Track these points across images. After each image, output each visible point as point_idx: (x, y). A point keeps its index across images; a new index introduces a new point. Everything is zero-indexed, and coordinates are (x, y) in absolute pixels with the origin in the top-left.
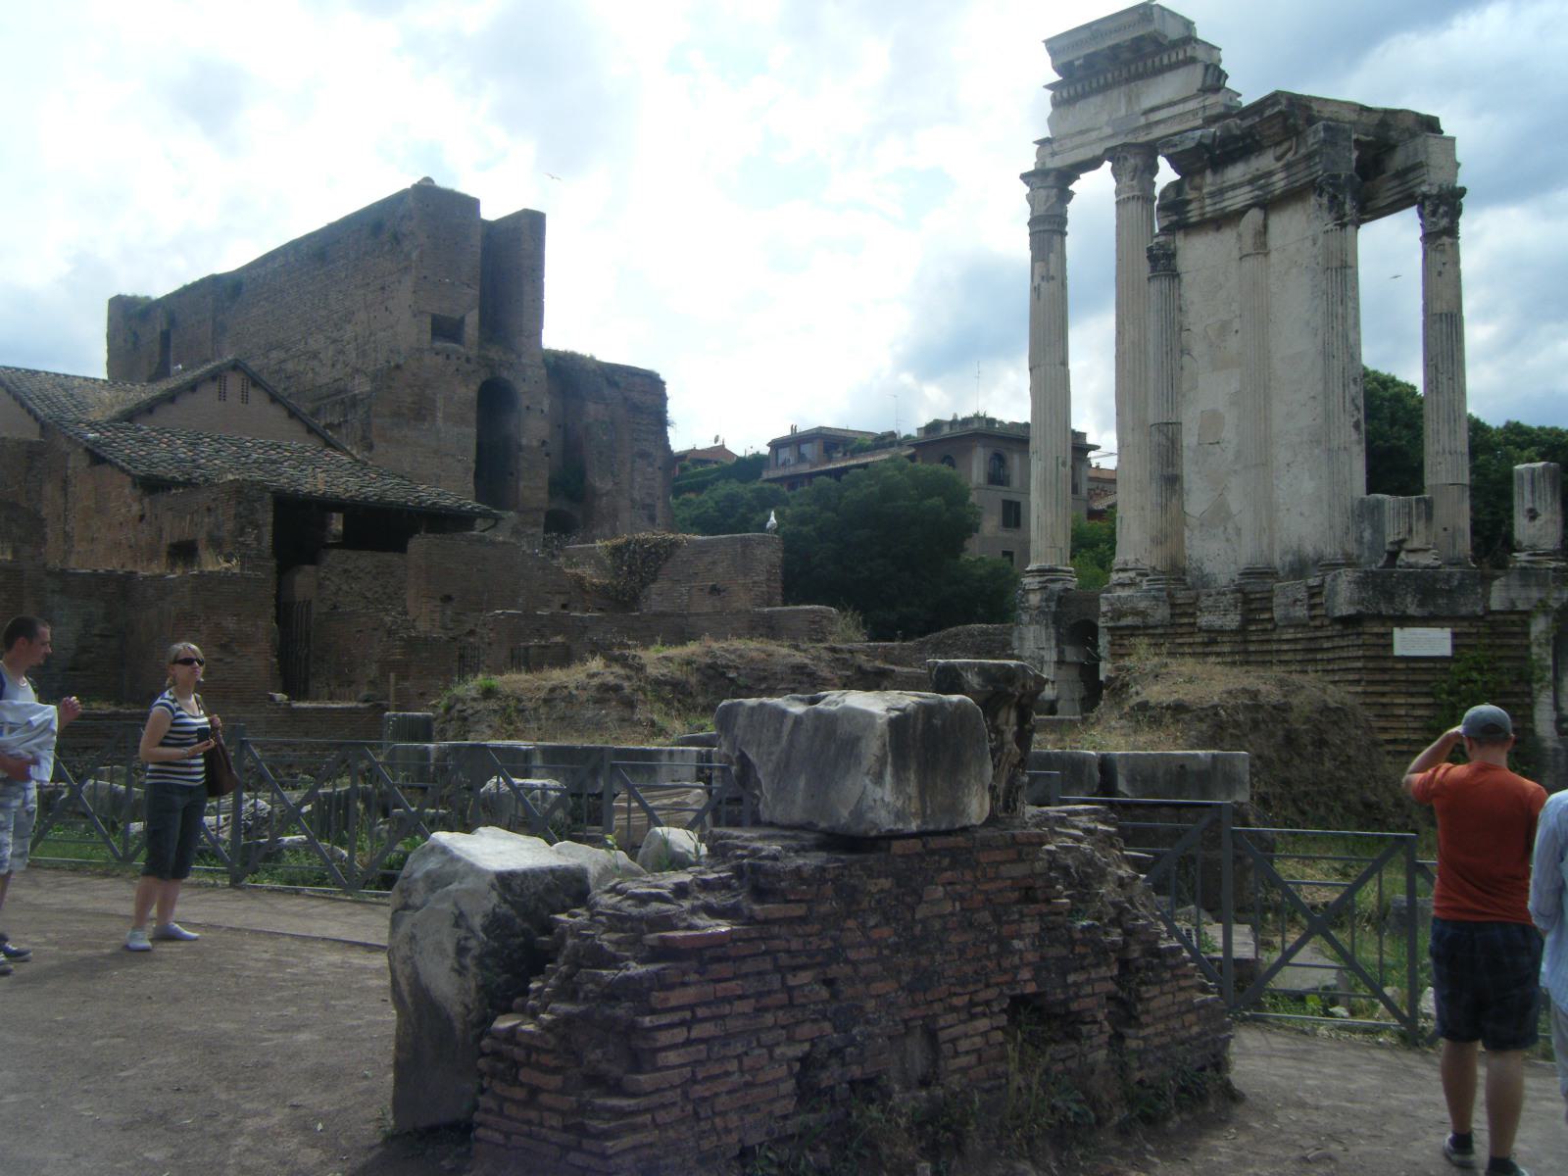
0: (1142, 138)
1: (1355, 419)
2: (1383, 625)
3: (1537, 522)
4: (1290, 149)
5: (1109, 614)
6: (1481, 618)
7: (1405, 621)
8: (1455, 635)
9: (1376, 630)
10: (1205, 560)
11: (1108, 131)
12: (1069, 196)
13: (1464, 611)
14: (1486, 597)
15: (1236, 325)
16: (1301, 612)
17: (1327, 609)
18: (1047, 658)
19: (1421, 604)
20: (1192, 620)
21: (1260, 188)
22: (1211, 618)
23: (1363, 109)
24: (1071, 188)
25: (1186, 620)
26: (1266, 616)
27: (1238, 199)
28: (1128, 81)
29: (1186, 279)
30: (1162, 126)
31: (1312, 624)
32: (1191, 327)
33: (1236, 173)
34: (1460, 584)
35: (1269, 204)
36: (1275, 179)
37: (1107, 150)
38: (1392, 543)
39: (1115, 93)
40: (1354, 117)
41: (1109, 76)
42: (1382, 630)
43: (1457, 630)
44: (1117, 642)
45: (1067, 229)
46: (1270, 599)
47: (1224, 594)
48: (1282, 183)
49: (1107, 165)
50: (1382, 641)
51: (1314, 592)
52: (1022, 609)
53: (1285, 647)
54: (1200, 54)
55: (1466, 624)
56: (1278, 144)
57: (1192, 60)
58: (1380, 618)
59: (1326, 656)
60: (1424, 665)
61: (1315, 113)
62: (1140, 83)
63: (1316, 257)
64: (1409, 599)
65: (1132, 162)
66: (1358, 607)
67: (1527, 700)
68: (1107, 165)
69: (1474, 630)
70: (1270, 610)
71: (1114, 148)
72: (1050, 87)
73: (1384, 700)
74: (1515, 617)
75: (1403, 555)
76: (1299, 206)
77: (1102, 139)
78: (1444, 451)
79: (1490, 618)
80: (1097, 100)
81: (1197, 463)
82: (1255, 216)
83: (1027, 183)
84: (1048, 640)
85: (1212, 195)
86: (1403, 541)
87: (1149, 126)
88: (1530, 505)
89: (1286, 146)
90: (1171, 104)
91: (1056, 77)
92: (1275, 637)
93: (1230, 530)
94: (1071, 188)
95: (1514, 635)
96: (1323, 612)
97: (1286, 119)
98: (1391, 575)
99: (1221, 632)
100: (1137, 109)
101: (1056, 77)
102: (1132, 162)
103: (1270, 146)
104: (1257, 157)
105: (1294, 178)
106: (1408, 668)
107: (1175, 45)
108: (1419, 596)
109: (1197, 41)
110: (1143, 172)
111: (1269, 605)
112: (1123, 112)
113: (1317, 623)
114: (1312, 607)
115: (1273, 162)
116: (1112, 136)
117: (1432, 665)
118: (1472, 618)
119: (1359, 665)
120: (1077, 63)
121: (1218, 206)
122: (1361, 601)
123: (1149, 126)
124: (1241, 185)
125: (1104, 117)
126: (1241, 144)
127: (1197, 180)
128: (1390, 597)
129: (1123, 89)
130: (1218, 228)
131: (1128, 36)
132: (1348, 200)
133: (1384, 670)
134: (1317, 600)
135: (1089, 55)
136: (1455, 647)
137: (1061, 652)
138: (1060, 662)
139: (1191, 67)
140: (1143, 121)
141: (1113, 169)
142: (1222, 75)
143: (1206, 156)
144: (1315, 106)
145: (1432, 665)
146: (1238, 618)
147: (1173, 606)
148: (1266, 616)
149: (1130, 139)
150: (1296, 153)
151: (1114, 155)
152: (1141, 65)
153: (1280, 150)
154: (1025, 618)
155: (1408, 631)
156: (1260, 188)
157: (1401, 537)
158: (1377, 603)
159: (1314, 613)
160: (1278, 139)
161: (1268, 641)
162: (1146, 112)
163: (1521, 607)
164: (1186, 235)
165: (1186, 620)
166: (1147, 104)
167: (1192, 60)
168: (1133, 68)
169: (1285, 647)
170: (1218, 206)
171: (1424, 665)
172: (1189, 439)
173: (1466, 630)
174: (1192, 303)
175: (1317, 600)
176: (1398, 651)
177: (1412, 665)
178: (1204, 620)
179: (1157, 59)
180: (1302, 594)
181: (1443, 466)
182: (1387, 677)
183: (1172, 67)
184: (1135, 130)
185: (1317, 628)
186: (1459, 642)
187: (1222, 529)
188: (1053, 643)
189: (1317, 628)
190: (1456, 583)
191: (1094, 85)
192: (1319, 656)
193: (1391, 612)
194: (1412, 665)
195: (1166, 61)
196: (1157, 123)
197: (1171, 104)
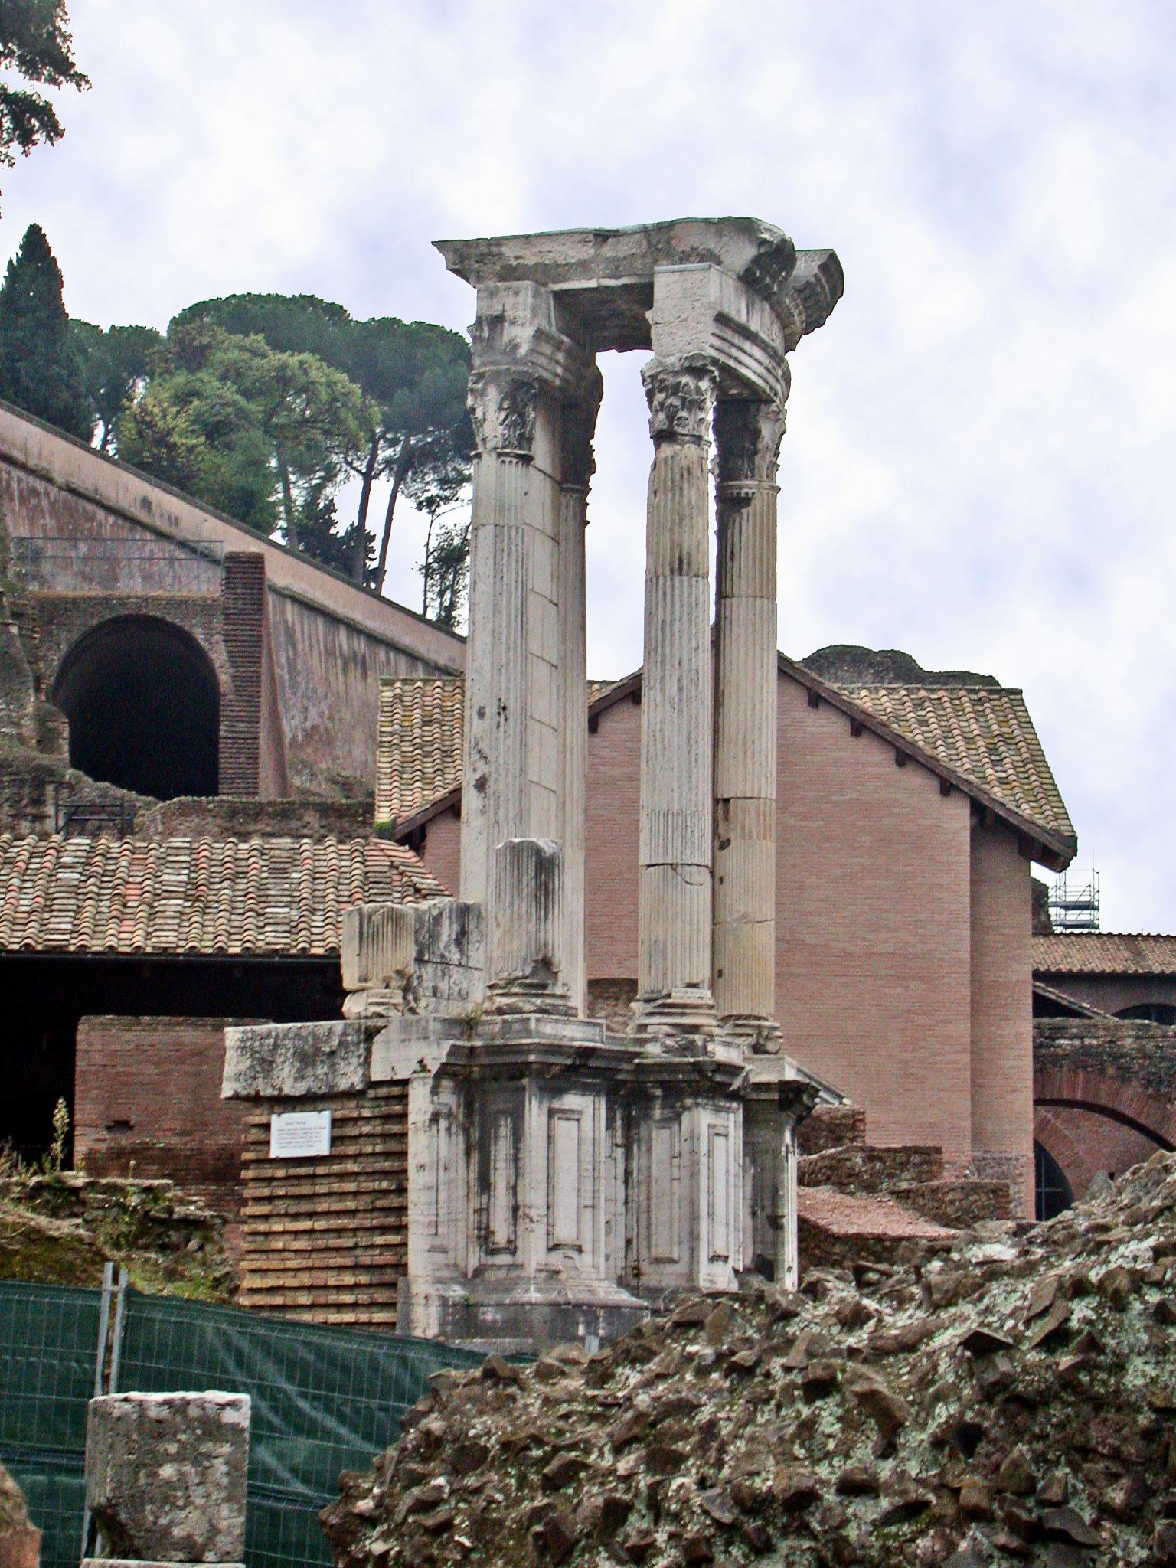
1: (478, 775)
6: (361, 1094)
8: (335, 1122)
13: (343, 1085)
19: (300, 1077)
34: (341, 1044)
42: (264, 1120)
43: (339, 1114)
58: (256, 1100)
60: (302, 1171)
64: (287, 1067)
73: (263, 1227)
79: (371, 1093)
117: (309, 1170)
118: (350, 1094)
136: (335, 1141)
155: (287, 1117)
158: (255, 1078)
163: (401, 1075)
171: (302, 1171)
176: (275, 1152)
182: (266, 1192)
186: (338, 1132)
190: (337, 1042)
193: (268, 1092)
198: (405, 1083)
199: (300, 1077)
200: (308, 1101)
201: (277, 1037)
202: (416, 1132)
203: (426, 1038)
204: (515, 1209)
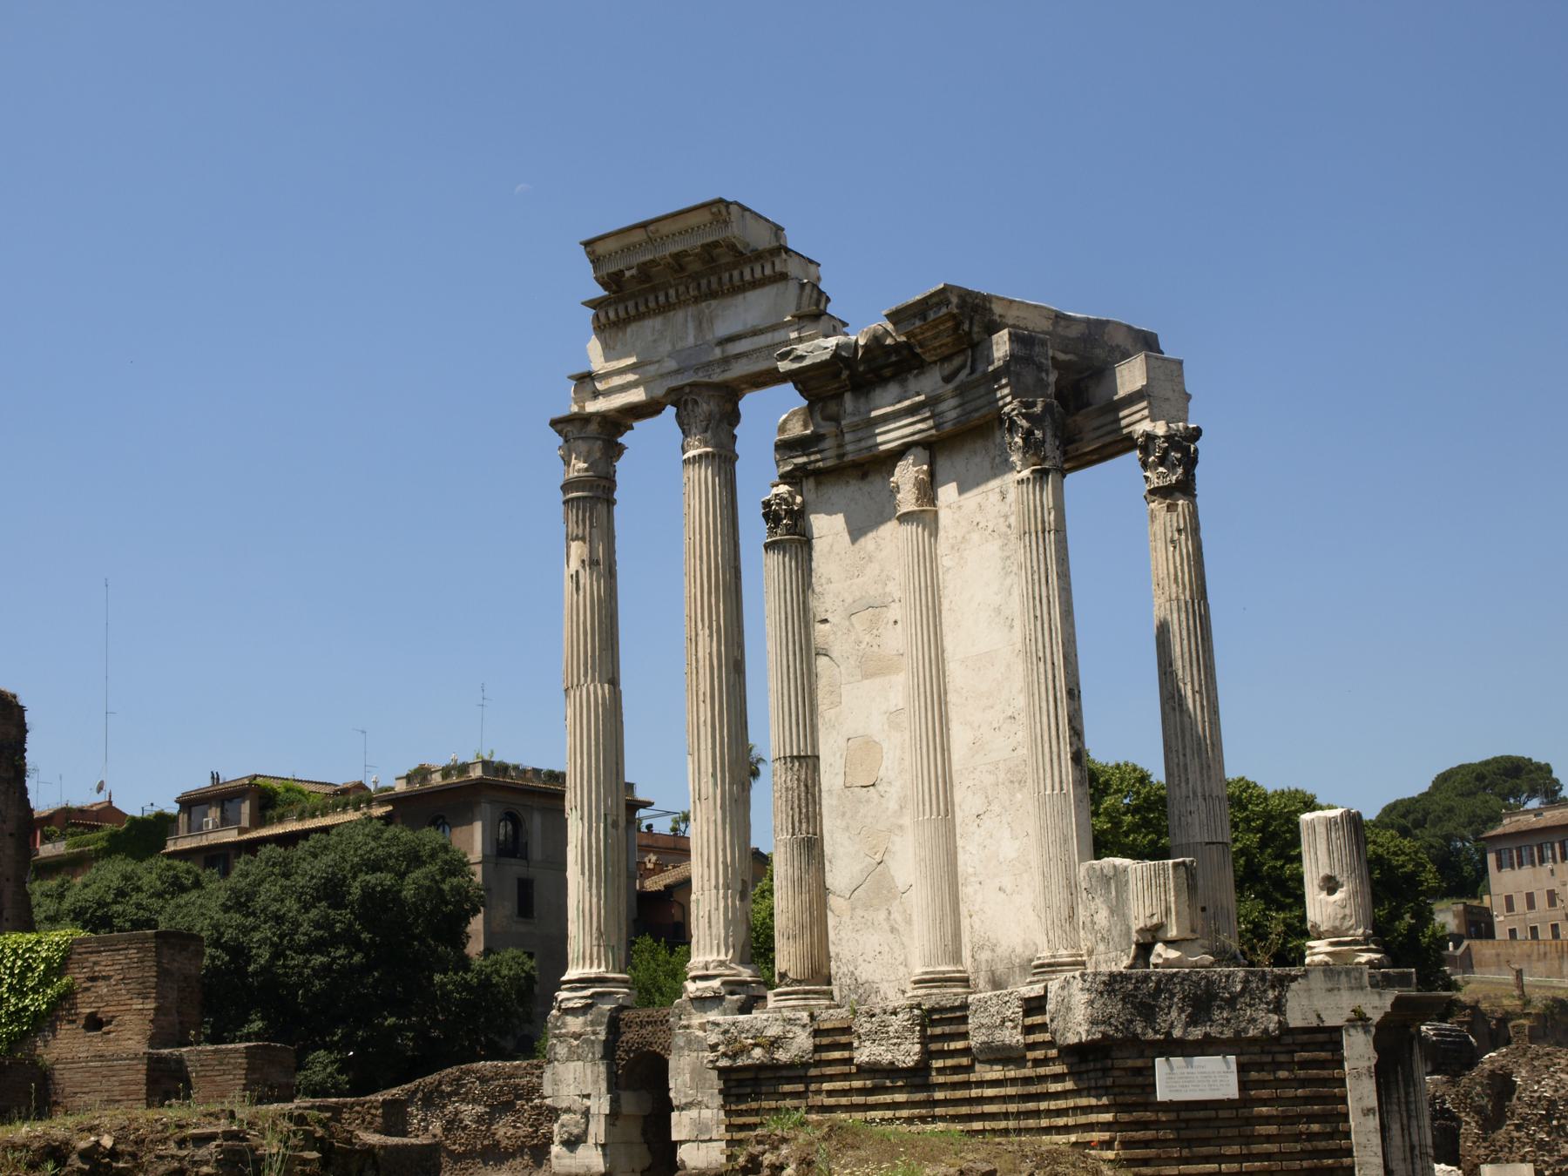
0: (717, 377)
2: (1141, 1055)
3: (1339, 895)
4: (963, 367)
5: (722, 1048)
6: (1277, 1039)
7: (1173, 1047)
8: (1242, 1069)
9: (1130, 1063)
10: (860, 960)
11: (671, 365)
12: (619, 450)
14: (1278, 1007)
15: (895, 612)
16: (1012, 1036)
17: (1054, 1033)
18: (593, 1110)
19: (1193, 1021)
20: (846, 1054)
22: (876, 1049)
23: (1059, 317)
24: (620, 440)
25: (837, 1055)
26: (960, 1045)
28: (697, 300)
30: (744, 360)
31: (1030, 1055)
32: (829, 616)
36: (943, 407)
37: (671, 391)
38: (1141, 931)
39: (679, 315)
40: (1046, 325)
41: (672, 292)
42: (1139, 1063)
43: (1245, 1059)
44: (734, 1091)
45: (616, 495)
46: (964, 1020)
47: (895, 1013)
48: (953, 414)
49: (670, 411)
50: (1140, 1080)
51: (1034, 1005)
52: (556, 1036)
53: (989, 1092)
54: (793, 268)
55: (1257, 1049)
57: (783, 277)
58: (1134, 1043)
59: (1053, 1105)
60: (1201, 1114)
61: (996, 318)
62: (714, 303)
63: (1006, 517)
65: (705, 407)
66: (1102, 1028)
67: (1347, 1161)
68: (670, 411)
69: (1269, 1059)
70: (965, 1036)
71: (681, 388)
72: (594, 304)
74: (1321, 1037)
75: (1159, 948)
77: (662, 376)
78: (1195, 793)
79: (1288, 1039)
80: (655, 323)
81: (844, 814)
83: (560, 433)
84: (596, 1082)
85: (855, 428)
86: (1160, 927)
87: (726, 361)
88: (1327, 871)
89: (957, 362)
90: (755, 333)
91: (599, 292)
92: (973, 1077)
93: (896, 916)
94: (620, 440)
95: (1321, 1064)
96: (1047, 1037)
97: (958, 326)
98: (1147, 978)
99: (892, 1071)
100: (709, 337)
101: (599, 292)
102: (705, 407)
103: (935, 362)
104: (916, 376)
105: (969, 407)
106: (1178, 1120)
107: (759, 256)
108: (1189, 1010)
109: (787, 251)
110: (720, 421)
111: (962, 1028)
112: (691, 340)
113: (1039, 1054)
115: (941, 383)
116: (677, 372)
117: (1212, 1114)
119: (1108, 1117)
120: (628, 274)
121: (863, 444)
122: (1106, 1021)
123: (726, 361)
125: (665, 347)
126: (894, 359)
127: (832, 408)
128: (1147, 1011)
129: (692, 310)
130: (864, 476)
131: (695, 242)
132: (1049, 439)
133: (1145, 1125)
134: (1038, 1019)
135: (644, 264)
136: (1243, 1085)
137: (614, 1103)
138: (613, 1117)
139: (780, 286)
140: (718, 352)
141: (678, 416)
142: (821, 297)
143: (845, 374)
144: (997, 309)
145: (1212, 1114)
146: (917, 1048)
147: (817, 1033)
148: (960, 1045)
149: (700, 377)
150: (973, 371)
151: (681, 399)
152: (714, 280)
153: (948, 368)
154: (561, 1050)
157: (1155, 920)
158: (1131, 1021)
159: (1031, 1038)
160: (947, 352)
161: (967, 1085)
162: (724, 341)
164: (818, 484)
165: (837, 1055)
166: (722, 329)
167: (783, 277)
168: (704, 282)
169: (989, 1092)
170: (863, 444)
171: (1201, 1114)
172: (830, 777)
173: (1256, 1058)
174: (830, 581)
175: (1038, 1019)
177: (1183, 1115)
178: (865, 1053)
179: (736, 273)
180: (1015, 1010)
181: (1195, 816)
183: (756, 284)
184: (710, 364)
185: (1037, 1063)
187: (882, 915)
188: (603, 1086)
189: (1037, 1063)
190: (1239, 988)
191: (652, 305)
192: (1043, 1105)
193: (1150, 1035)
194: (1183, 1115)
195: (747, 276)
196: (738, 356)
197: (755, 333)
198: (1338, 1029)
199: (1193, 1021)
200: (1206, 1046)
201: (1158, 982)
202: (1359, 1076)
203: (1362, 988)
204: (1412, 1148)
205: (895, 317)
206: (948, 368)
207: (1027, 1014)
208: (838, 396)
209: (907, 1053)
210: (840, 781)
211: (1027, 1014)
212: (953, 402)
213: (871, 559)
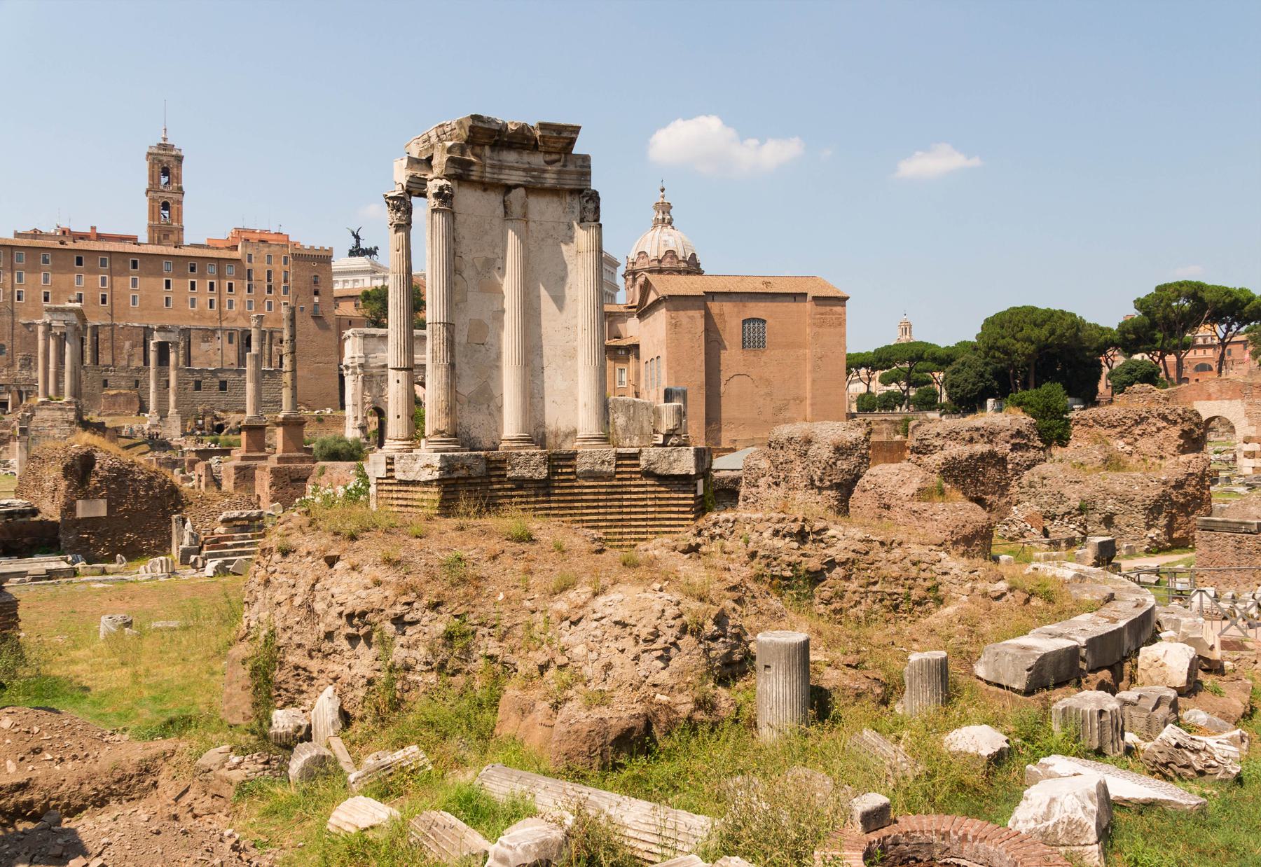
4: (559, 160)
21: (533, 177)
26: (569, 470)
27: (513, 177)
29: (459, 218)
33: (510, 157)
35: (533, 189)
36: (547, 175)
46: (574, 459)
56: (550, 153)
59: (634, 496)
76: (556, 199)
82: (521, 191)
89: (554, 157)
99: (531, 480)
114: (617, 466)
124: (517, 169)
130: (485, 190)
148: (569, 470)
153: (549, 158)
156: (533, 177)
172: (461, 338)
185: (619, 479)
205: (543, 126)
206: (549, 158)
207: (618, 459)
208: (483, 145)
209: (543, 473)
210: (464, 340)
211: (618, 459)
212: (554, 176)
213: (486, 233)
